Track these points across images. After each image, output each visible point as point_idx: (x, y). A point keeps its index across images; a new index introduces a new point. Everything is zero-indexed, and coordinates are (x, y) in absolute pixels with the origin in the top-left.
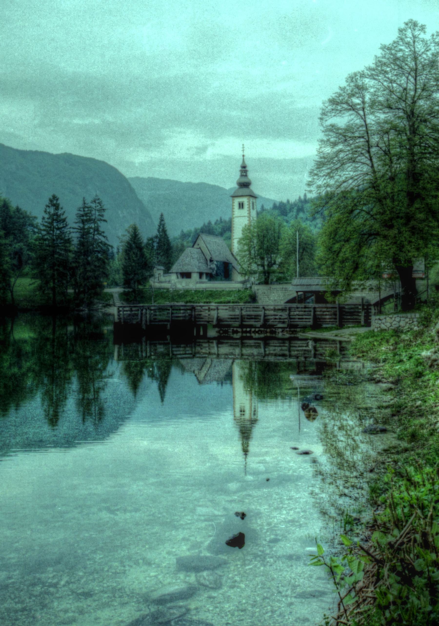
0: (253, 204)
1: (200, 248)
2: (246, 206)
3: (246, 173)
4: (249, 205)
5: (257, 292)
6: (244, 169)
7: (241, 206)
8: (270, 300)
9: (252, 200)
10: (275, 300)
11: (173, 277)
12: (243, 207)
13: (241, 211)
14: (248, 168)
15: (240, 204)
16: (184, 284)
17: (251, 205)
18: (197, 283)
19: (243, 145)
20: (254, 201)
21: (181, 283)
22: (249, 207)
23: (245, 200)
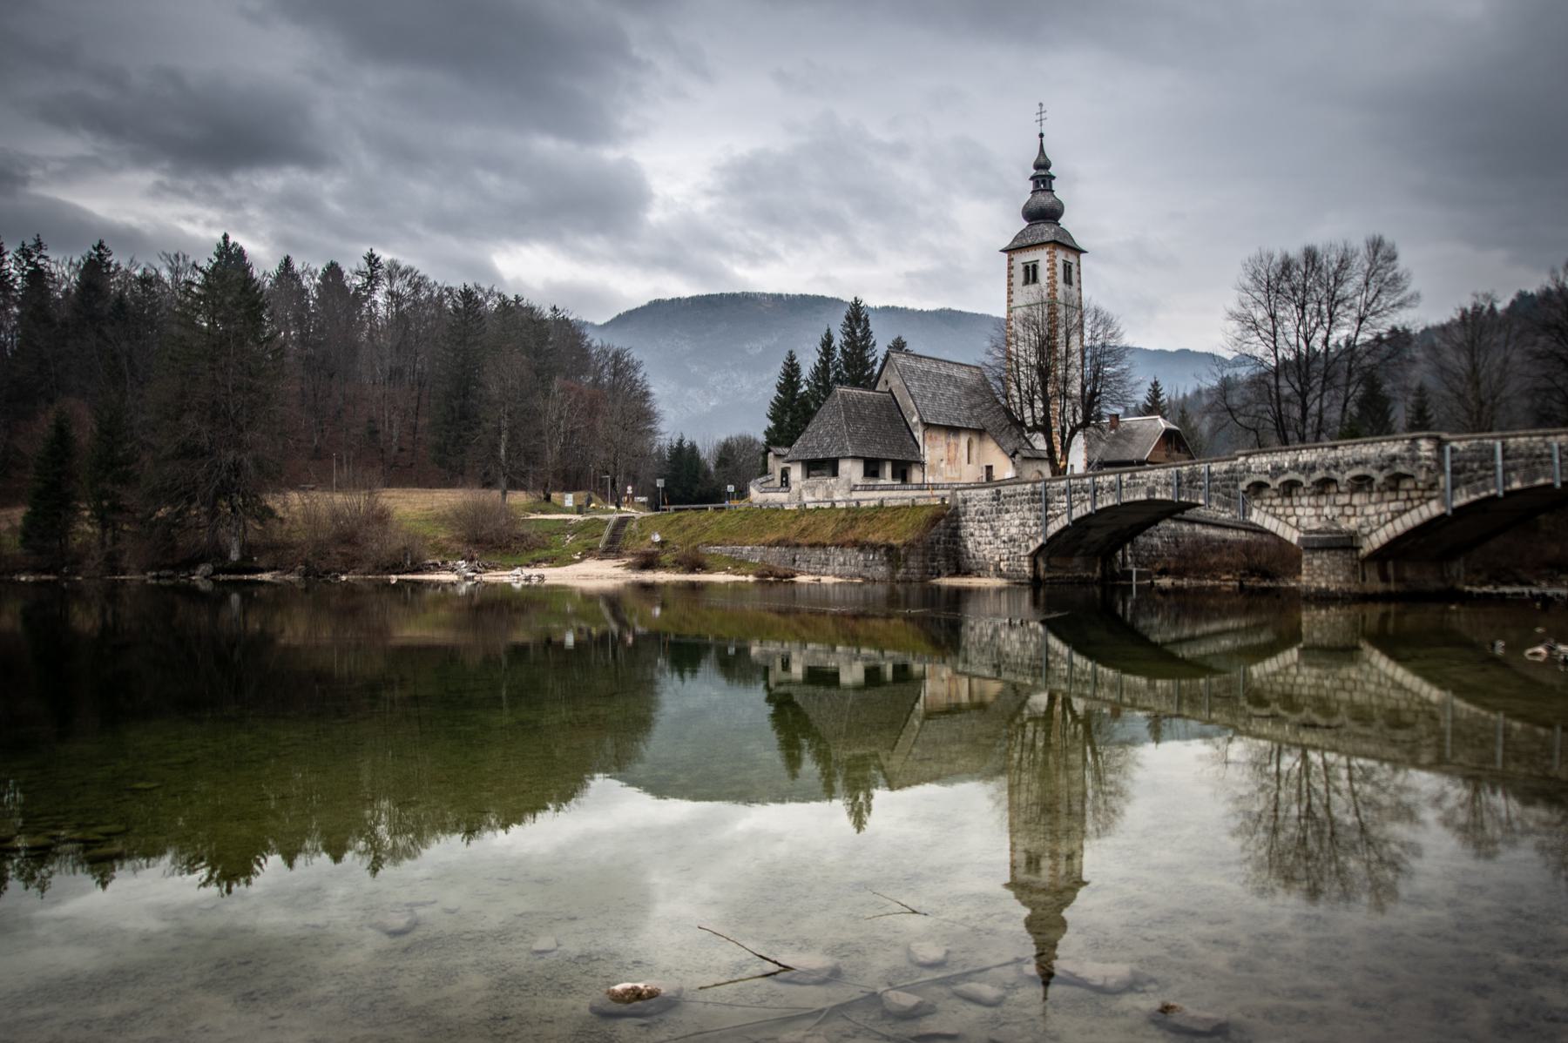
0: (1067, 268)
1: (890, 391)
2: (1043, 275)
3: (1051, 186)
4: (1052, 269)
5: (962, 510)
6: (1043, 177)
7: (1031, 274)
8: (996, 536)
9: (1061, 256)
10: (1012, 540)
11: (796, 473)
12: (1035, 280)
13: (1032, 288)
14: (1052, 171)
15: (1027, 268)
16: (820, 495)
17: (1060, 270)
18: (854, 489)
19: (1041, 105)
20: (1072, 258)
21: (812, 489)
22: (1052, 277)
23: (1041, 257)
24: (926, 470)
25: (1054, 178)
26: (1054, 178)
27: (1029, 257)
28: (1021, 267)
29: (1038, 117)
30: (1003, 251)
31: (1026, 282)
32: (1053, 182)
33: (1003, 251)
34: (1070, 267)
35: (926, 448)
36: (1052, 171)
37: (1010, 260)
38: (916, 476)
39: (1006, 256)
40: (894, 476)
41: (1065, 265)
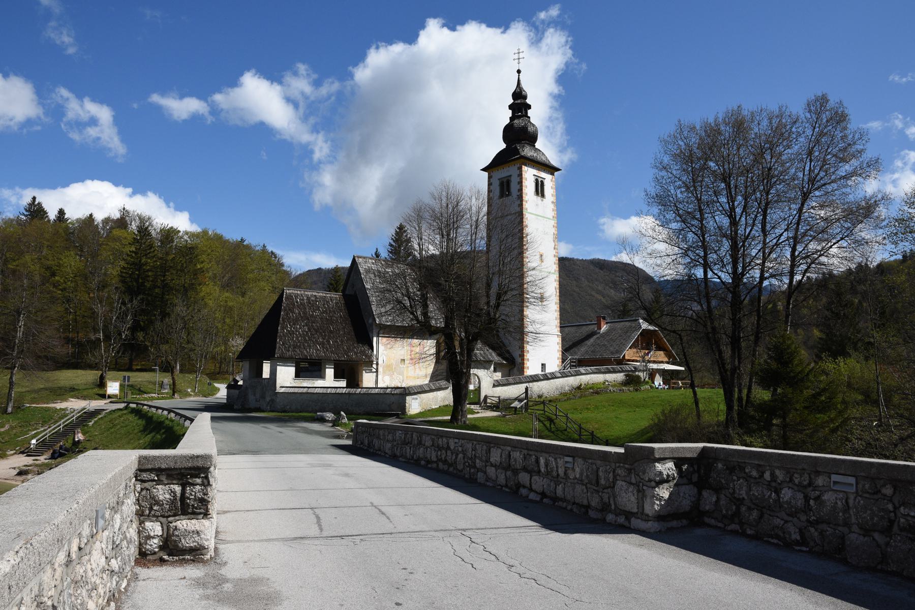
3: (527, 113)
24: (380, 369)
25: (529, 107)
26: (529, 107)
27: (502, 173)
28: (498, 183)
29: (516, 56)
30: (484, 170)
31: (502, 195)
32: (529, 111)
33: (484, 170)
34: (542, 183)
35: (381, 348)
36: (528, 101)
37: (490, 178)
38: (368, 380)
39: (486, 174)
40: (337, 376)
41: (537, 180)
